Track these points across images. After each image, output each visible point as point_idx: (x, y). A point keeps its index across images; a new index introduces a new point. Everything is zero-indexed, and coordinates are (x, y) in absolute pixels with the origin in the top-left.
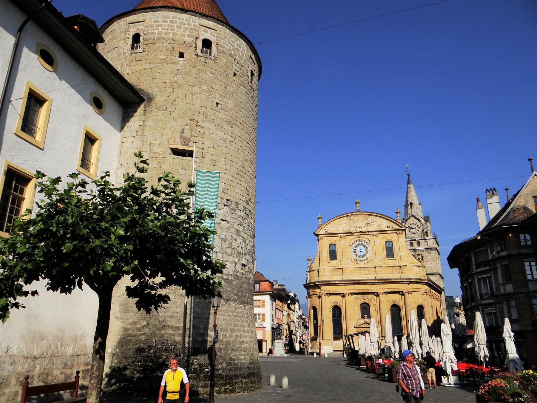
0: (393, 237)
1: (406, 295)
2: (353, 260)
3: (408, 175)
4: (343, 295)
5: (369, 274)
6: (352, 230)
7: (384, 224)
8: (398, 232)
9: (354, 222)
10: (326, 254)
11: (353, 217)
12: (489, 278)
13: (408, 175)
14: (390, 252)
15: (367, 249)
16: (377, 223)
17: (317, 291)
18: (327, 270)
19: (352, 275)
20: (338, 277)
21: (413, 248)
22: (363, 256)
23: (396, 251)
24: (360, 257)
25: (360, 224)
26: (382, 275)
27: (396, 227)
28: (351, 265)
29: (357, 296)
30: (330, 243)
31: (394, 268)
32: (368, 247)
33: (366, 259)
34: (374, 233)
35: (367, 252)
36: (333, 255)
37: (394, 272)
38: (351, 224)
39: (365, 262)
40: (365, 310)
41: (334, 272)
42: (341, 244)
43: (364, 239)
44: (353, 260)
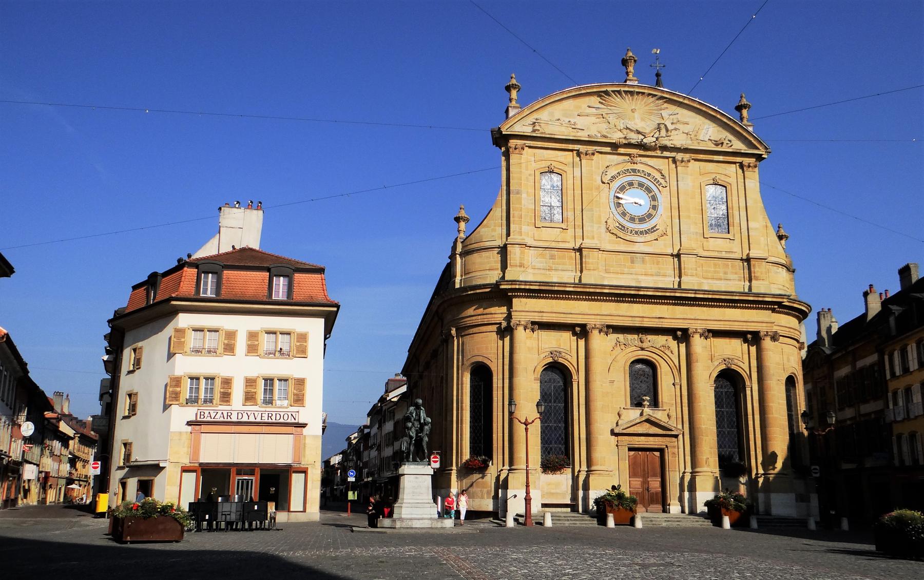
1: (767, 343)
2: (612, 225)
4: (581, 331)
5: (658, 275)
6: (616, 137)
8: (746, 161)
9: (620, 116)
11: (617, 99)
15: (654, 198)
16: (686, 129)
17: (498, 313)
18: (532, 252)
19: (607, 271)
20: (565, 275)
22: (642, 220)
24: (632, 219)
25: (638, 123)
26: (697, 279)
28: (608, 242)
29: (621, 337)
31: (729, 262)
33: (653, 230)
34: (679, 156)
35: (654, 207)
37: (730, 276)
38: (612, 118)
39: (649, 237)
40: (644, 382)
41: (552, 257)
43: (648, 170)
44: (612, 225)
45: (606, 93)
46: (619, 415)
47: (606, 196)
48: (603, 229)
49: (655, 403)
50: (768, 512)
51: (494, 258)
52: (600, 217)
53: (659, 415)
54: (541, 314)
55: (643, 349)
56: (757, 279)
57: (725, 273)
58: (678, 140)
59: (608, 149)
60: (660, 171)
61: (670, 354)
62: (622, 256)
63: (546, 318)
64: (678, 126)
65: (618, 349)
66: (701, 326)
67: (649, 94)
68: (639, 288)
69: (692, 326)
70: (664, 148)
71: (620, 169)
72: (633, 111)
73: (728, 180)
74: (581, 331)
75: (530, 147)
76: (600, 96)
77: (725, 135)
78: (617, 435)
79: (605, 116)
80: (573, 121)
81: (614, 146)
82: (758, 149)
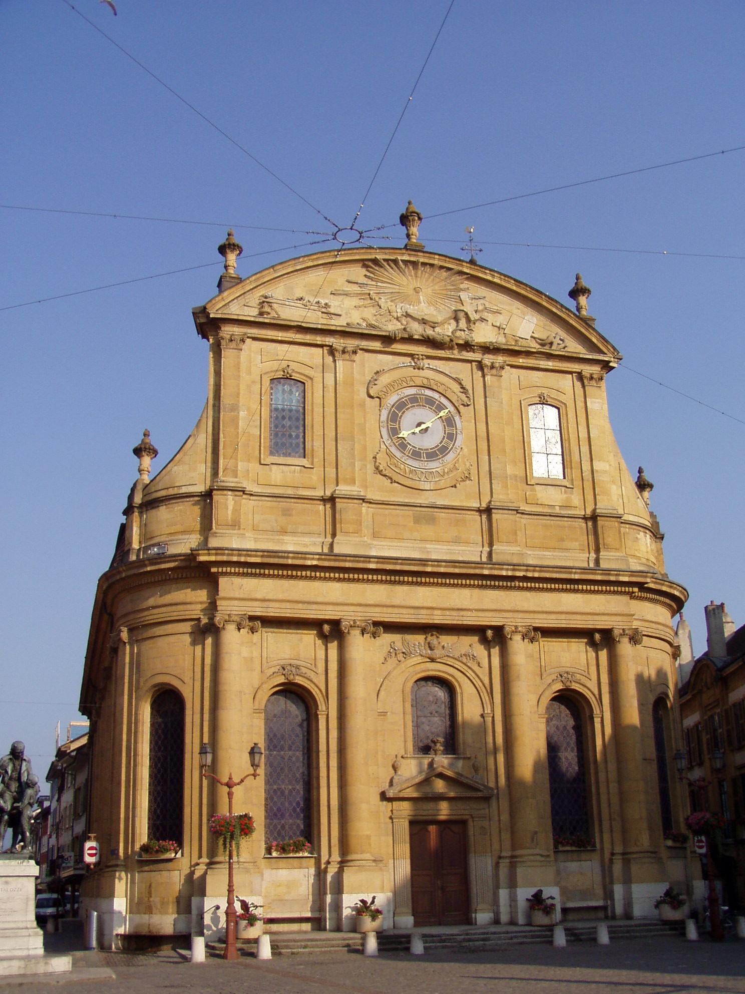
1: (625, 648)
4: (332, 631)
5: (457, 541)
6: (392, 327)
8: (587, 370)
9: (396, 297)
11: (391, 273)
16: (499, 320)
17: (194, 598)
19: (375, 535)
20: (305, 541)
25: (423, 309)
26: (518, 548)
28: (377, 489)
29: (396, 638)
30: (273, 367)
32: (457, 418)
35: (451, 437)
37: (568, 544)
41: (286, 513)
45: (375, 262)
46: (395, 768)
47: (373, 419)
48: (370, 468)
50: (628, 916)
51: (190, 513)
52: (365, 448)
54: (265, 604)
55: (433, 660)
56: (607, 548)
57: (562, 540)
58: (483, 334)
59: (377, 345)
60: (458, 381)
61: (475, 668)
62: (400, 511)
63: (273, 611)
64: (485, 315)
65: (392, 661)
66: (524, 622)
67: (441, 267)
68: (423, 562)
69: (508, 621)
70: (467, 346)
71: (396, 375)
72: (417, 290)
73: (562, 398)
74: (332, 631)
75: (254, 339)
76: (365, 266)
77: (555, 332)
78: (390, 800)
79: (374, 296)
80: (323, 302)
81: (388, 340)
82: (601, 352)
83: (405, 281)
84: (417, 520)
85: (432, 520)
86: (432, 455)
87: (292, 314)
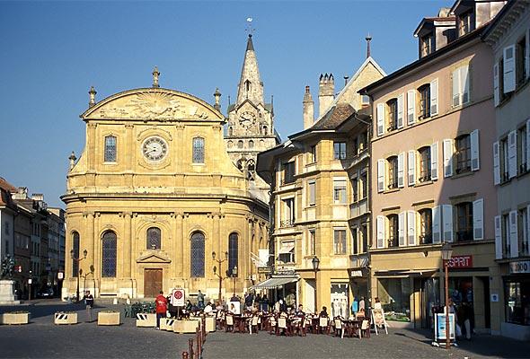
0: (207, 131)
3: (250, 36)
6: (144, 117)
7: (190, 109)
9: (147, 105)
10: (100, 151)
12: (293, 199)
13: (250, 36)
14: (199, 155)
15: (164, 147)
21: (243, 150)
23: (208, 153)
25: (157, 108)
27: (212, 117)
35: (164, 152)
36: (110, 154)
42: (123, 135)
49: (158, 246)
53: (160, 253)
83: (151, 98)
84: (151, 179)
85: (156, 179)
86: (157, 158)
87: (111, 115)
